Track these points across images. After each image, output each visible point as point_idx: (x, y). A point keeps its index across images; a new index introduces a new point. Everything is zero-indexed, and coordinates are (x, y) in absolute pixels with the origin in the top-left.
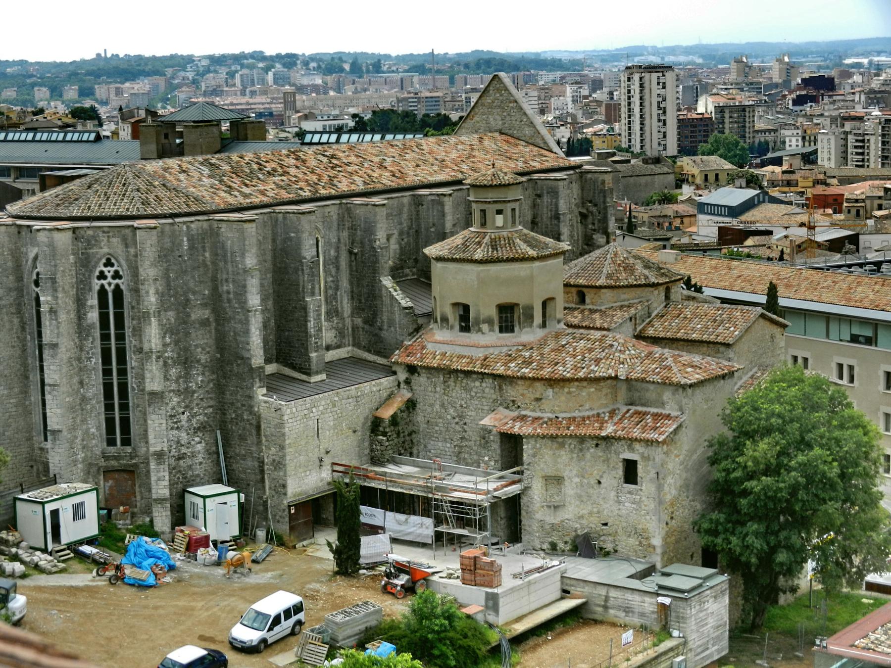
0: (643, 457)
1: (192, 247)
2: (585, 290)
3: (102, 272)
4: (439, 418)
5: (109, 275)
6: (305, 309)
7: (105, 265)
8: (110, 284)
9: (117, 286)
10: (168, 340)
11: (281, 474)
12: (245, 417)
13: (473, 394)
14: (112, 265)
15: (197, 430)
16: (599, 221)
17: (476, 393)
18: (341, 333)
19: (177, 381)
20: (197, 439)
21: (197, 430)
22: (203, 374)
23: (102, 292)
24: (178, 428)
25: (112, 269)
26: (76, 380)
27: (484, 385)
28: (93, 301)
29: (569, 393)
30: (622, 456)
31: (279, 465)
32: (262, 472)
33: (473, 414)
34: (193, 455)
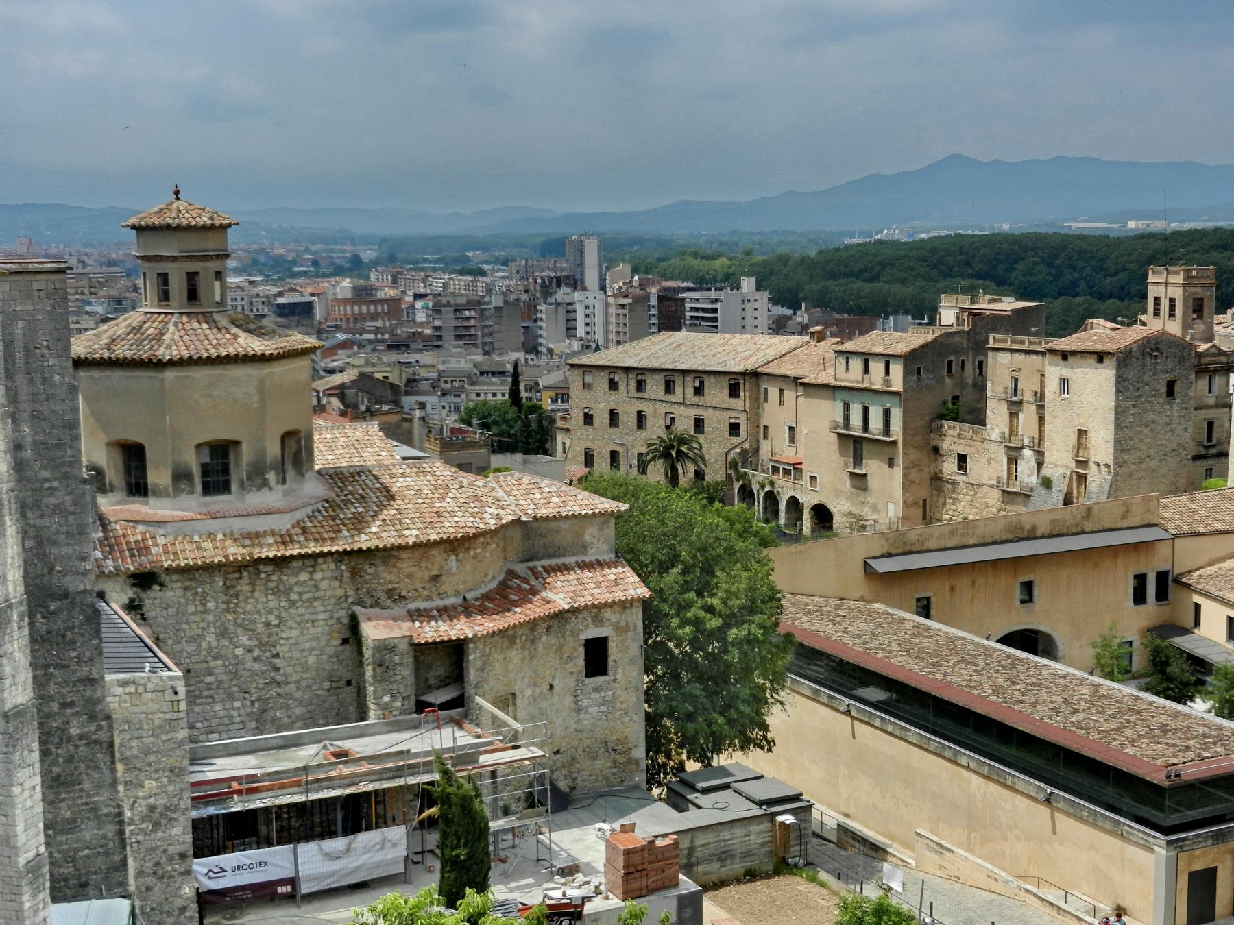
0: (618, 628)
4: (216, 658)
12: (74, 731)
13: (294, 597)
17: (300, 594)
27: (318, 576)
29: (475, 557)
30: (583, 637)
32: (123, 843)
33: (295, 633)
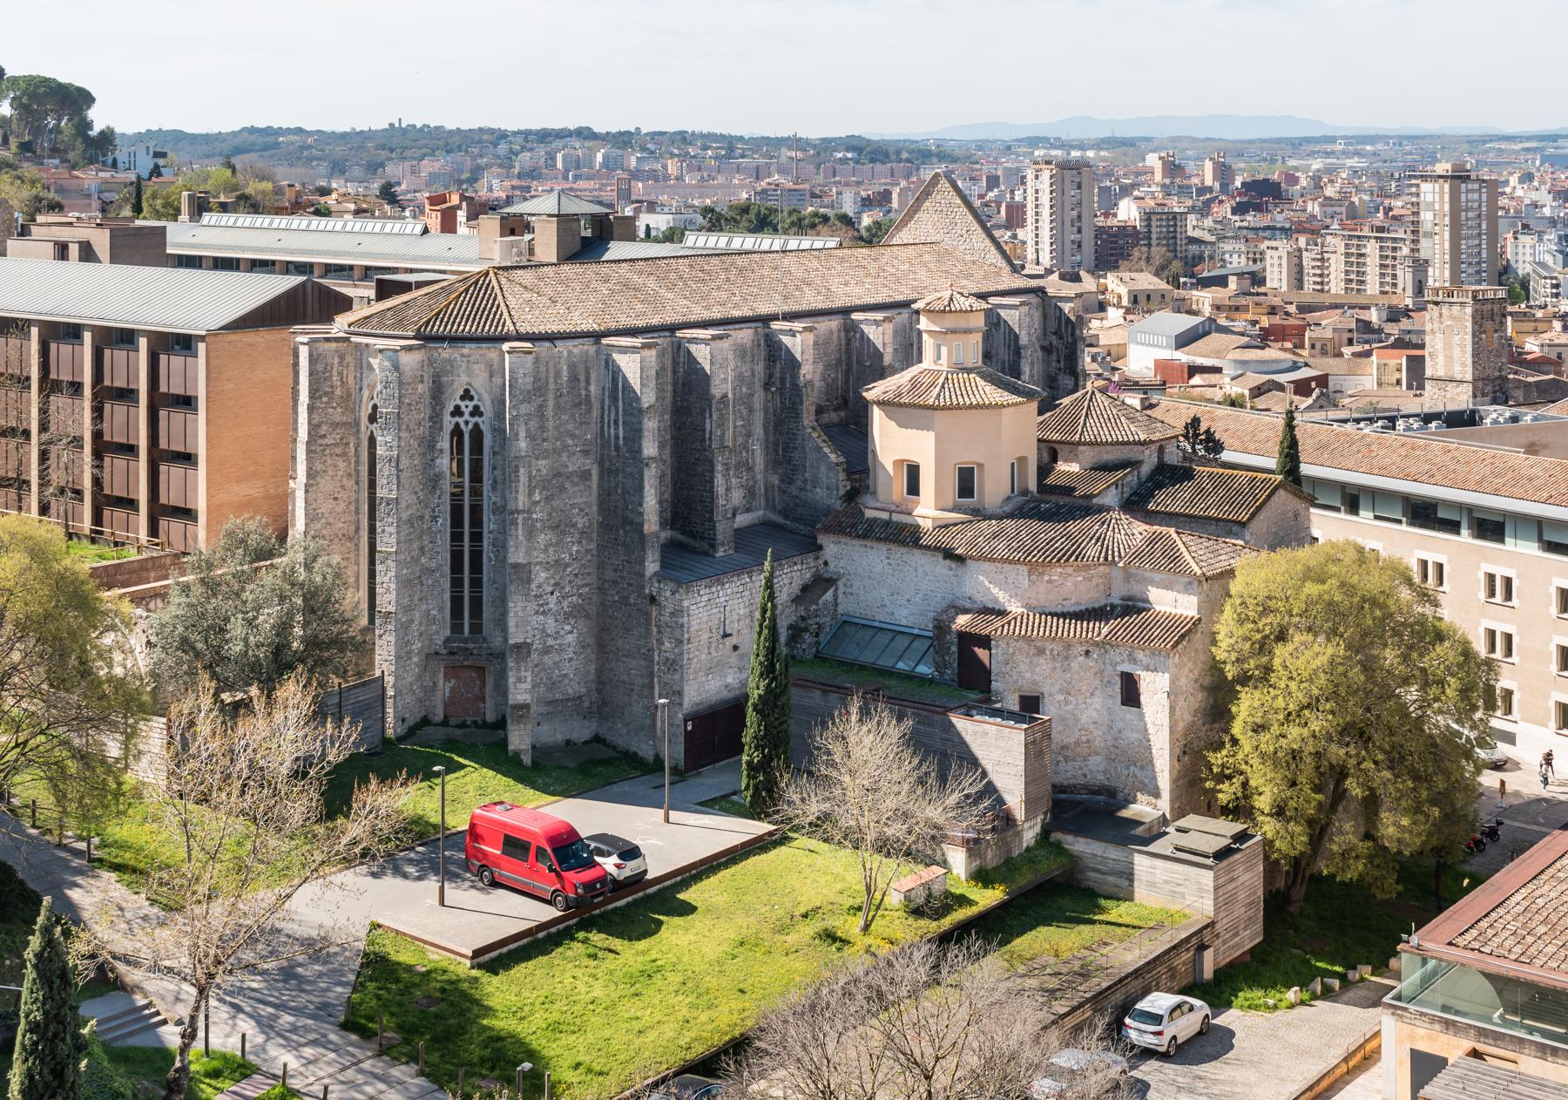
1: (574, 378)
2: (1057, 446)
3: (457, 408)
5: (467, 412)
6: (712, 464)
7: (462, 398)
8: (467, 423)
9: (476, 425)
10: (537, 497)
11: (677, 677)
14: (471, 398)
15: (568, 616)
16: (1066, 358)
18: (751, 492)
19: (546, 551)
20: (568, 628)
21: (568, 616)
22: (580, 542)
23: (457, 432)
24: (544, 613)
25: (471, 404)
26: (415, 545)
28: (444, 443)
30: (1120, 668)
31: (674, 665)
32: (651, 675)
34: (561, 650)
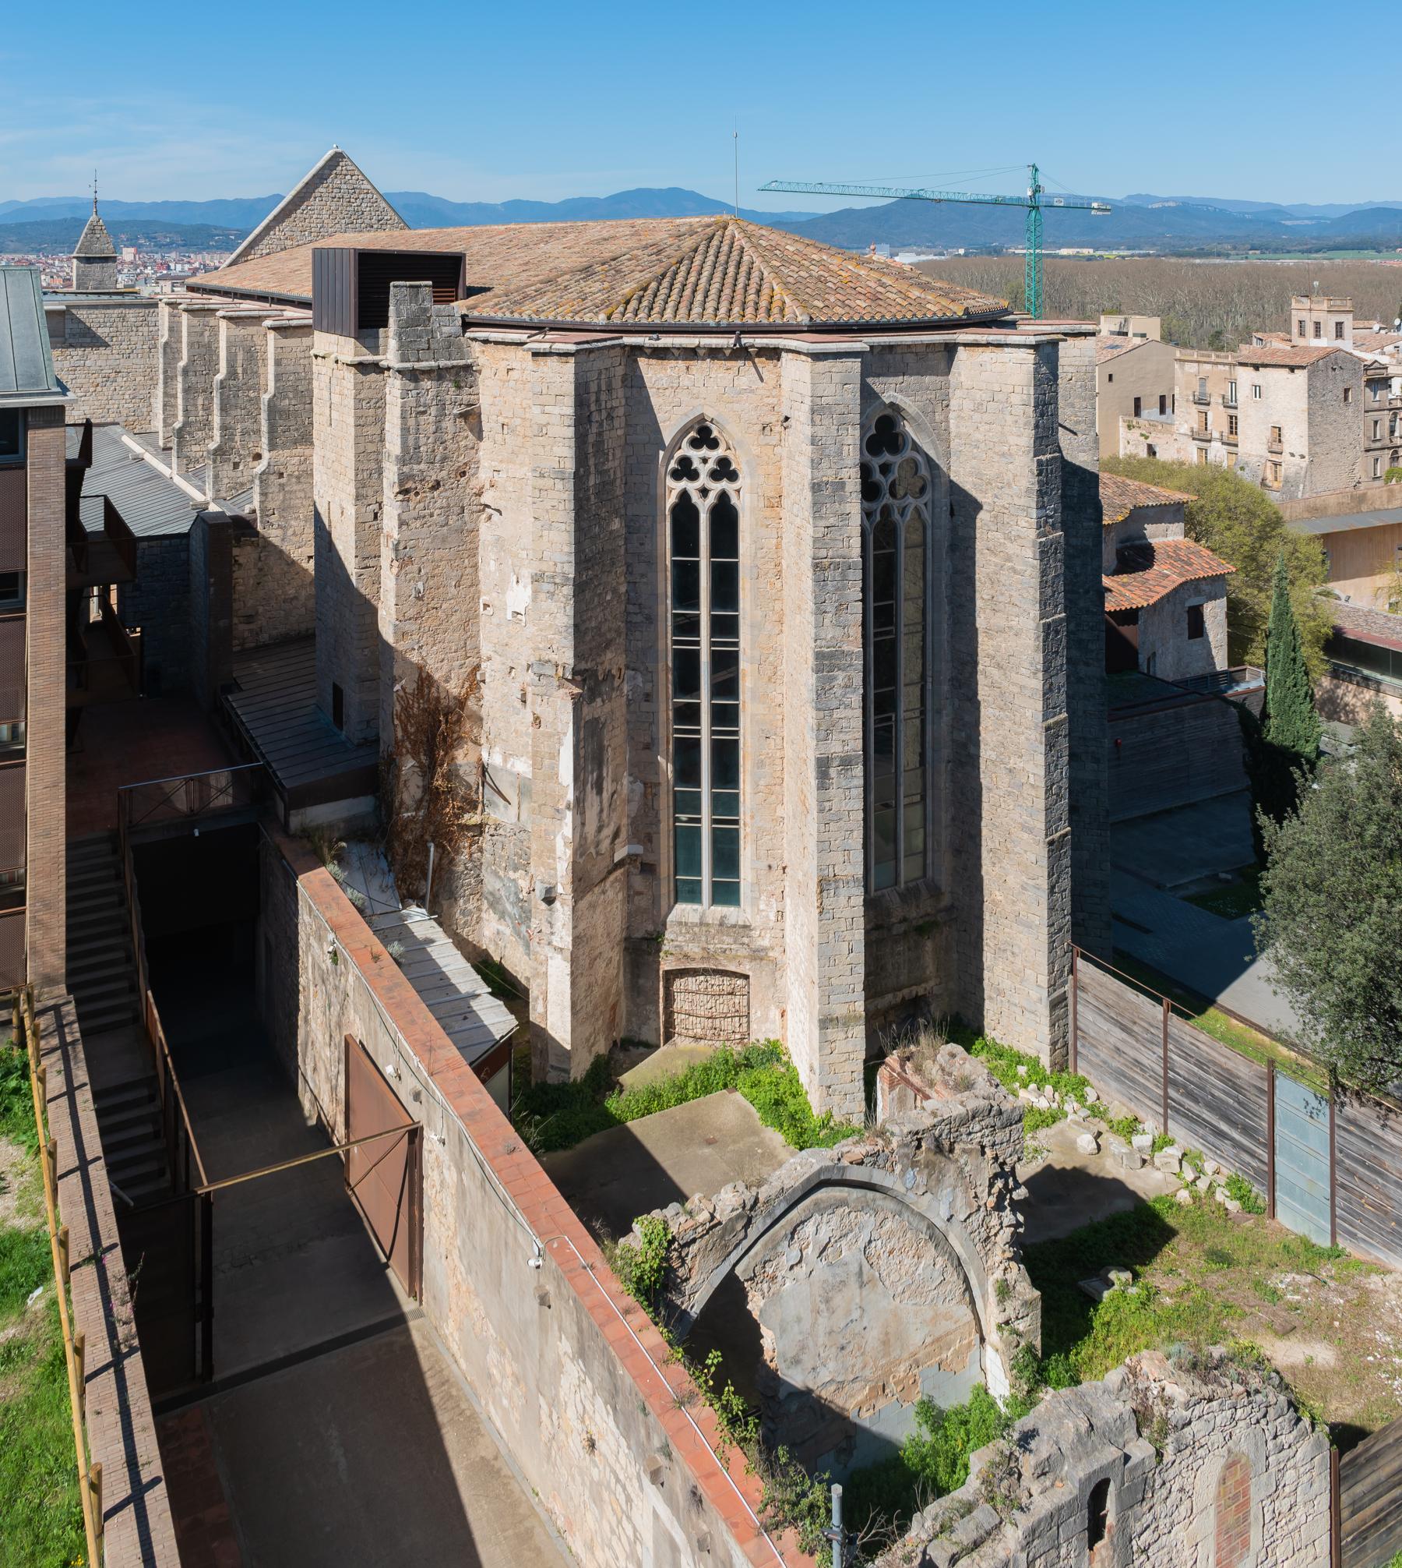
3: (685, 462)
5: (704, 470)
8: (704, 492)
9: (723, 496)
14: (714, 444)
